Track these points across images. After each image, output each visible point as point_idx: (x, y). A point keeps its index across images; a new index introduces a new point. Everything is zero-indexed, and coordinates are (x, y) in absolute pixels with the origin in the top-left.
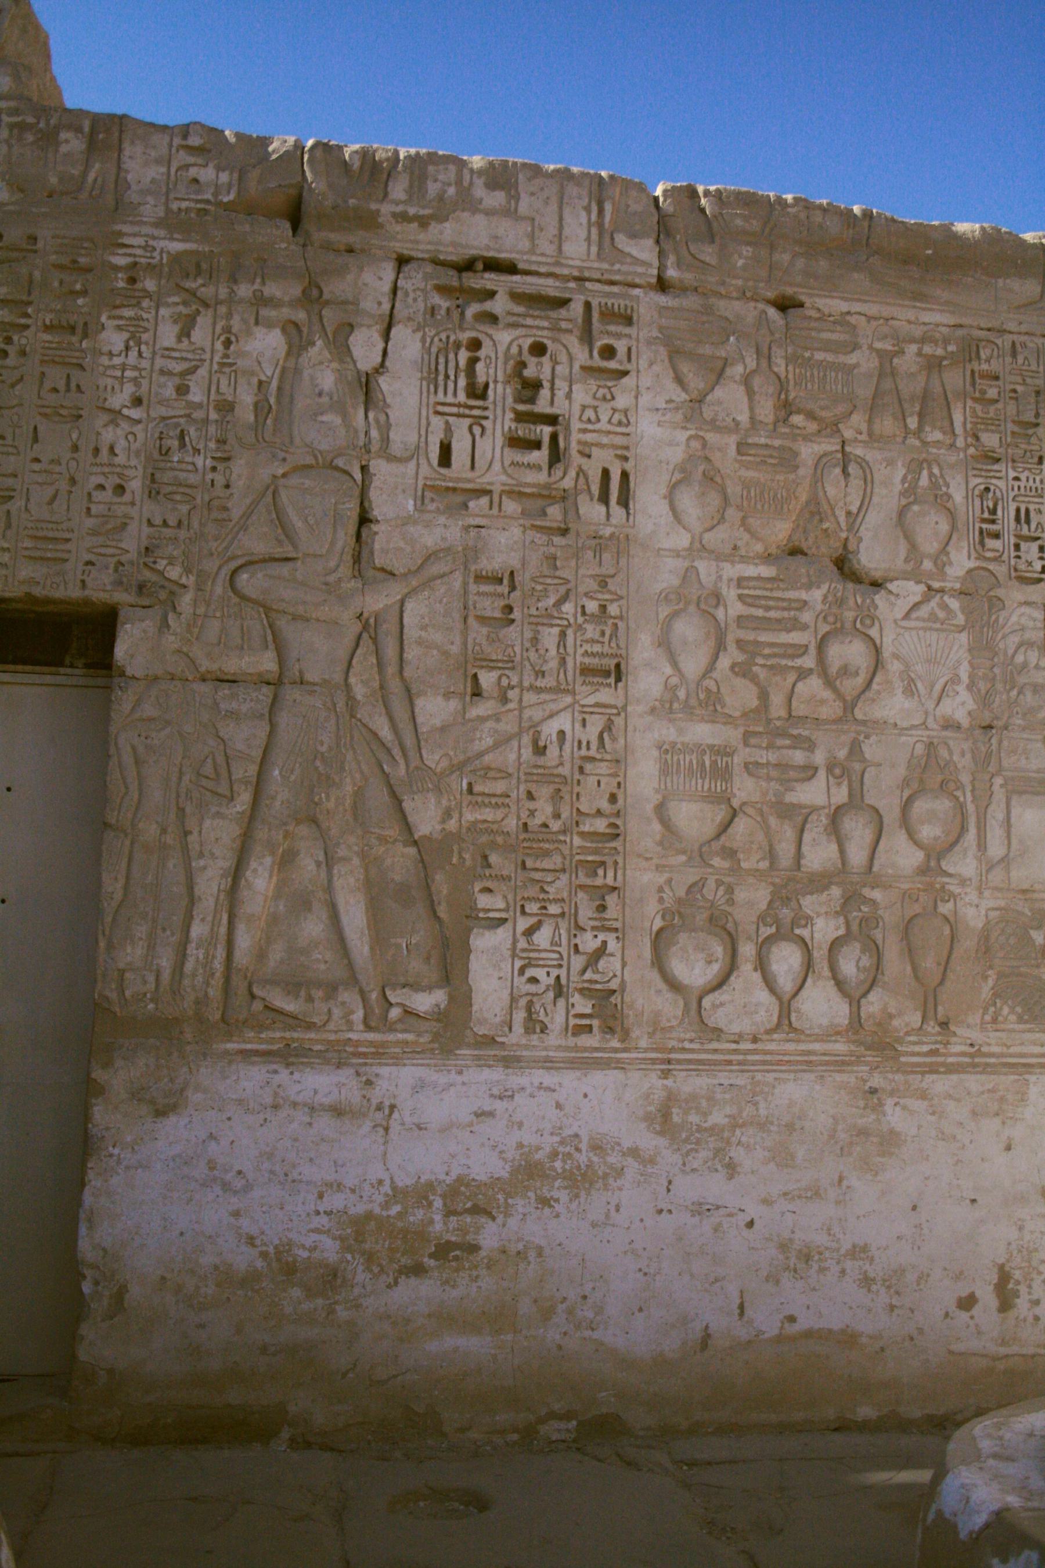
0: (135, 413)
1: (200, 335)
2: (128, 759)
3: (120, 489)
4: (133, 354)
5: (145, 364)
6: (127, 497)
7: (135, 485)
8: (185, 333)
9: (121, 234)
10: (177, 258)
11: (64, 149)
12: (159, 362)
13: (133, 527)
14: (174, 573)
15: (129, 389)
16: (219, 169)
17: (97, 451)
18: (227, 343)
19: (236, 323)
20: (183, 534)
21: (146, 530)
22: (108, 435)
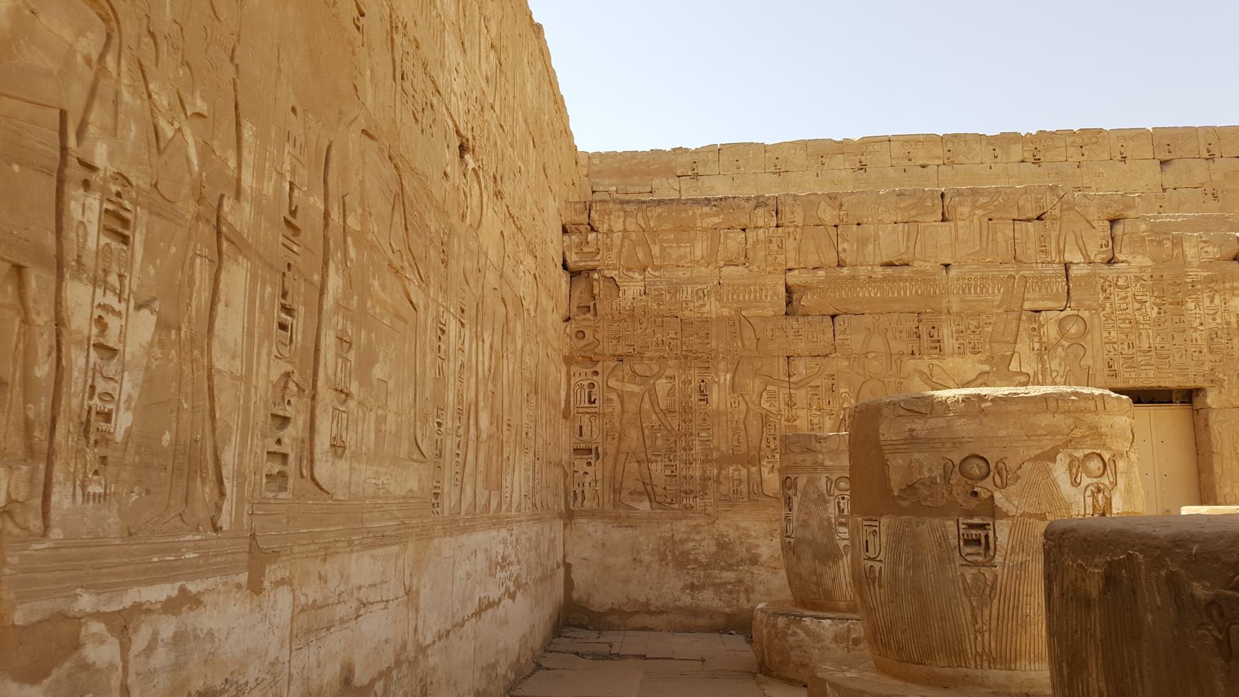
0: (1201, 328)
1: (1217, 300)
2: (1216, 433)
3: (1201, 352)
4: (1198, 309)
5: (1202, 312)
6: (1203, 354)
7: (1205, 350)
8: (1212, 301)
9: (1188, 272)
10: (1205, 278)
11: (1165, 246)
12: (1206, 311)
13: (1206, 363)
14: (1221, 376)
15: (1198, 320)
16: (1213, 247)
17: (1192, 341)
18: (1225, 303)
19: (1227, 296)
20: (1222, 364)
21: (1211, 364)
22: (1195, 335)
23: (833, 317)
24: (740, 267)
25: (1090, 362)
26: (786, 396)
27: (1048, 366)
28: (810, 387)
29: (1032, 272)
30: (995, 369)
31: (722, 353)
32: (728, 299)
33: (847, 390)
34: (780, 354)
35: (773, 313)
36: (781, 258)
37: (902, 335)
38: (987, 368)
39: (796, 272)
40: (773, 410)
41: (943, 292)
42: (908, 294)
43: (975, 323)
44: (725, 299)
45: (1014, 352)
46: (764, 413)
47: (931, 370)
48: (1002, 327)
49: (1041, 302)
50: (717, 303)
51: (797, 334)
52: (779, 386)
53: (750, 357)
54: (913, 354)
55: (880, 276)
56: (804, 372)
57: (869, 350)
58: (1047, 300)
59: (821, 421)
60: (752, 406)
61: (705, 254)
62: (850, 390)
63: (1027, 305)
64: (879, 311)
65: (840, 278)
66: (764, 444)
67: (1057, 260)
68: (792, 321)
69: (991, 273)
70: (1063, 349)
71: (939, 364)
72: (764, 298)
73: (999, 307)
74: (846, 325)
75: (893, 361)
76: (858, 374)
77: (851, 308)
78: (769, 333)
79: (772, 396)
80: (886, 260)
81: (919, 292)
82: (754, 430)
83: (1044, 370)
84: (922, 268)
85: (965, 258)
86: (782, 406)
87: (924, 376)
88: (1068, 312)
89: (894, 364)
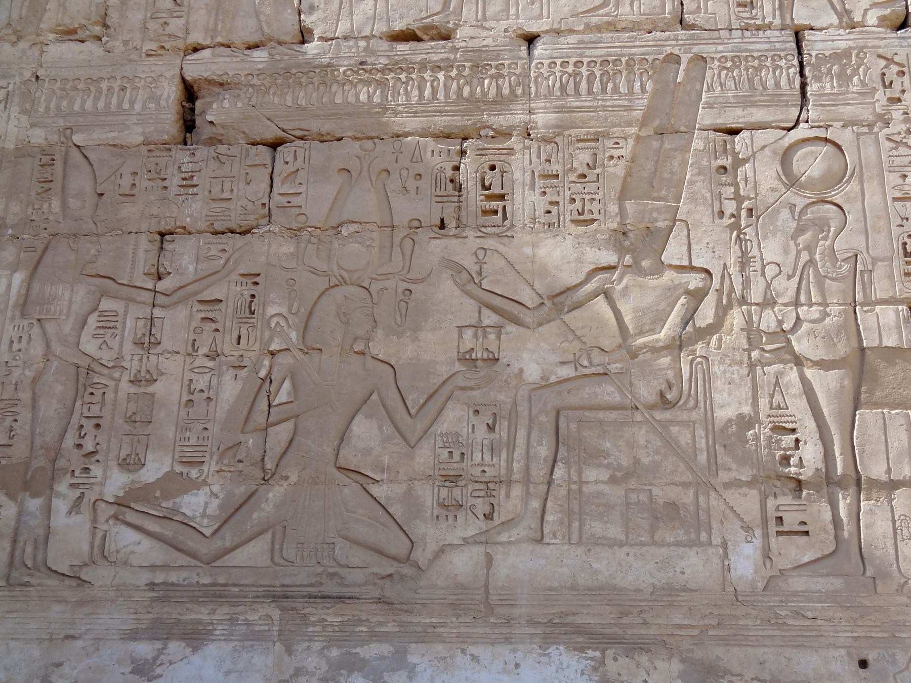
23: (274, 145)
24: (87, 43)
25: (858, 242)
26: (141, 323)
27: (755, 252)
28: (200, 302)
29: (720, 48)
30: (628, 259)
31: (12, 227)
32: (47, 108)
33: (284, 311)
34: (144, 227)
35: (141, 139)
36: (175, 26)
37: (420, 183)
38: (608, 257)
39: (206, 53)
40: (106, 357)
41: (519, 91)
42: (441, 96)
43: (585, 157)
44: (42, 110)
45: (675, 221)
46: (84, 362)
47: (480, 263)
48: (650, 166)
49: (739, 112)
50: (24, 118)
51: (188, 183)
52: (129, 300)
53: (75, 235)
54: (442, 226)
55: (384, 61)
56: (191, 268)
57: (345, 217)
58: (754, 105)
59: (214, 382)
60: (57, 348)
61: (15, 16)
62: (290, 311)
63: (705, 117)
64: (373, 134)
65: (299, 65)
66: (70, 440)
67: (777, 21)
68: (182, 156)
69: (625, 51)
70: (792, 212)
71: (500, 248)
72: (126, 106)
73: (643, 124)
74: (299, 163)
75: (397, 240)
76: (314, 271)
77: (315, 126)
78: (126, 181)
79: (108, 324)
80: (399, 26)
81: (466, 91)
82: (50, 409)
83: (744, 261)
84: (472, 44)
85: (570, 20)
86: (128, 347)
87: (465, 276)
88: (802, 131)
89: (397, 249)
